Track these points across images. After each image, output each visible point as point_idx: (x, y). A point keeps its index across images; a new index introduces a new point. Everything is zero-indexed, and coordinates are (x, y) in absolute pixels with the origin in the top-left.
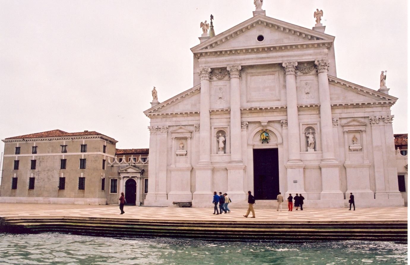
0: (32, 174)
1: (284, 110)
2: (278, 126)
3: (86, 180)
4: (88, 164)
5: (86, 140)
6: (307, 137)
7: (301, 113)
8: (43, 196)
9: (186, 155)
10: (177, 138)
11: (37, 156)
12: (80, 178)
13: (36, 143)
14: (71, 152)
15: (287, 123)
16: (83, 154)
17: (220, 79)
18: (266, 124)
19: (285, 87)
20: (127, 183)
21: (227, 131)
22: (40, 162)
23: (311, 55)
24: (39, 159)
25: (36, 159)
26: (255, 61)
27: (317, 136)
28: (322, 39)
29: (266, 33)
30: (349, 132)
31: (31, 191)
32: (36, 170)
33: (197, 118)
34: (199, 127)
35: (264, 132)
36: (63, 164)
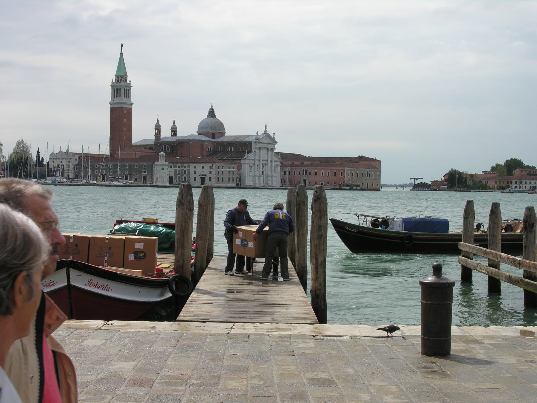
2: (265, 164)
4: (234, 173)
19: (267, 154)
33: (254, 161)
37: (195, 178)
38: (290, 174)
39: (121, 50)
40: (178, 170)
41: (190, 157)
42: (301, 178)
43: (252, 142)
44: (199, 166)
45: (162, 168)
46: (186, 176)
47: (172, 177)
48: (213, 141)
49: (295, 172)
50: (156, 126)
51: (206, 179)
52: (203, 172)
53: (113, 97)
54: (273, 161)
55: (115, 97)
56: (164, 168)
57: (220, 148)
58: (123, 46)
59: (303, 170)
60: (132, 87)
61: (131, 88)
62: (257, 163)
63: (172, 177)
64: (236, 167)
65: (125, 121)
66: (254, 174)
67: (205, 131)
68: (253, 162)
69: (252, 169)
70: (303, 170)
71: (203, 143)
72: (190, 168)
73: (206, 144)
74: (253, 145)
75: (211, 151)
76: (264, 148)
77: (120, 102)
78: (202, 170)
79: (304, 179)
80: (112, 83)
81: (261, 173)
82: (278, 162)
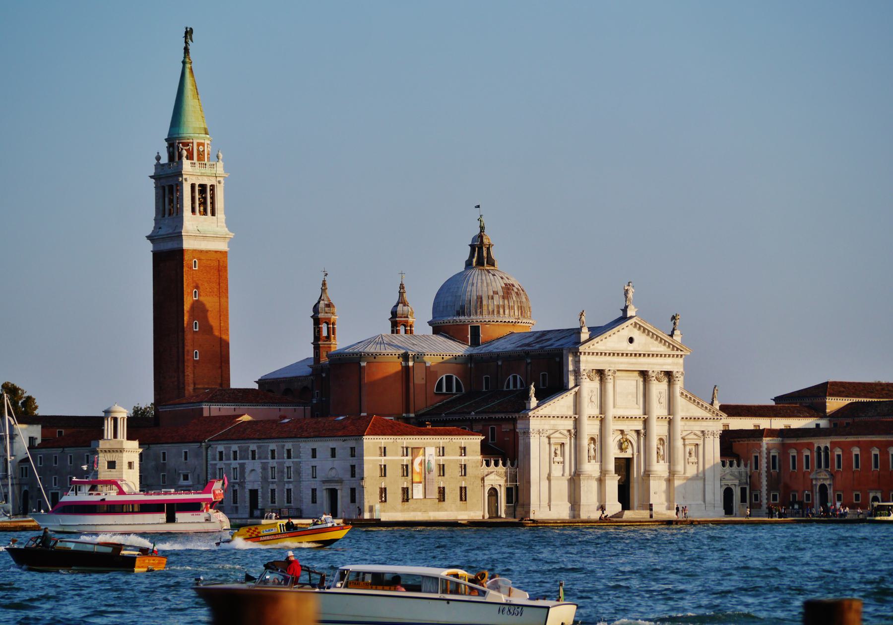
0: (405, 483)
2: (635, 435)
4: (468, 470)
5: (465, 441)
6: (658, 448)
8: (420, 511)
10: (556, 444)
12: (461, 488)
13: (406, 442)
14: (449, 455)
15: (645, 435)
16: (463, 458)
20: (490, 489)
23: (669, 365)
26: (626, 365)
28: (681, 351)
29: (636, 334)
30: (690, 444)
31: (406, 503)
35: (626, 441)
37: (314, 491)
38: (774, 467)
39: (186, 50)
40: (270, 465)
41: (362, 414)
42: (812, 480)
43: (565, 352)
44: (323, 446)
45: (109, 463)
46: (291, 486)
47: (257, 491)
49: (794, 457)
50: (316, 309)
51: (342, 497)
52: (334, 471)
53: (160, 216)
54: (678, 417)
55: (164, 216)
56: (114, 462)
57: (487, 378)
58: (193, 36)
59: (819, 448)
63: (257, 491)
66: (573, 470)
67: (446, 319)
69: (563, 455)
70: (819, 448)
72: (300, 457)
75: (454, 391)
76: (618, 370)
77: (176, 231)
78: (330, 463)
79: (821, 482)
80: (158, 166)
81: (611, 466)
82: (704, 423)
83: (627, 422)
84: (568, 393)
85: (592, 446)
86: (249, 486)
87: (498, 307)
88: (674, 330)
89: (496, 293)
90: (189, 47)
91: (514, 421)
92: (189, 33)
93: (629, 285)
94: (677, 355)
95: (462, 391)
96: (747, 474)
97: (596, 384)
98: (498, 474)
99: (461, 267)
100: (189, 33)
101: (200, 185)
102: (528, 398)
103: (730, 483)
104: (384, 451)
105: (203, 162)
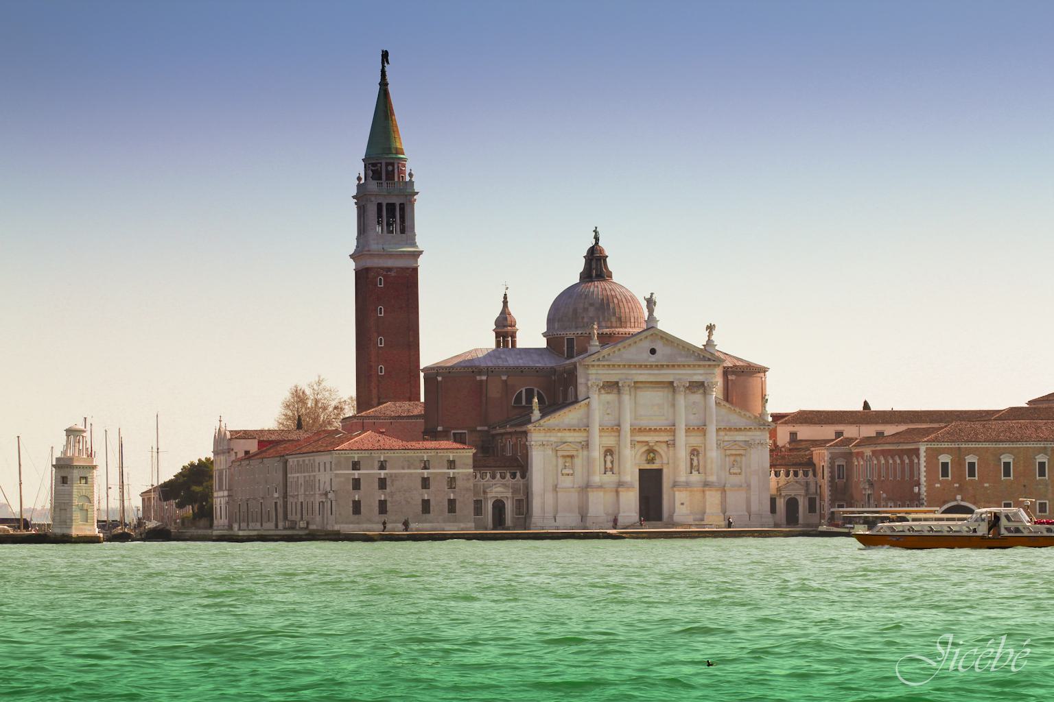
0: (383, 496)
1: (672, 429)
2: (664, 446)
3: (457, 502)
4: (459, 483)
6: (692, 459)
7: (688, 434)
9: (572, 475)
11: (387, 474)
13: (384, 457)
14: (434, 468)
16: (451, 471)
17: (608, 393)
18: (653, 444)
19: (673, 405)
21: (616, 450)
22: (393, 481)
23: (701, 374)
24: (391, 476)
25: (386, 476)
27: (701, 456)
31: (383, 515)
32: (388, 490)
33: (585, 434)
34: (588, 445)
36: (425, 483)
48: (537, 371)
54: (712, 429)
56: (66, 477)
60: (417, 193)
61: (415, 197)
62: (599, 442)
64: (470, 461)
65: (382, 315)
68: (579, 437)
71: (484, 378)
73: (503, 381)
74: (581, 380)
80: (359, 186)
81: (631, 476)
83: (652, 433)
84: (577, 406)
85: (609, 458)
86: (300, 501)
87: (591, 318)
88: (709, 339)
89: (591, 305)
90: (386, 69)
91: (525, 433)
92: (385, 55)
93: (651, 296)
94: (709, 366)
95: (545, 403)
96: (816, 484)
97: (611, 397)
98: (505, 486)
99: (578, 281)
100: (385, 55)
101: (387, 204)
102: (531, 410)
103: (793, 494)
104: (356, 466)
105: (393, 182)
